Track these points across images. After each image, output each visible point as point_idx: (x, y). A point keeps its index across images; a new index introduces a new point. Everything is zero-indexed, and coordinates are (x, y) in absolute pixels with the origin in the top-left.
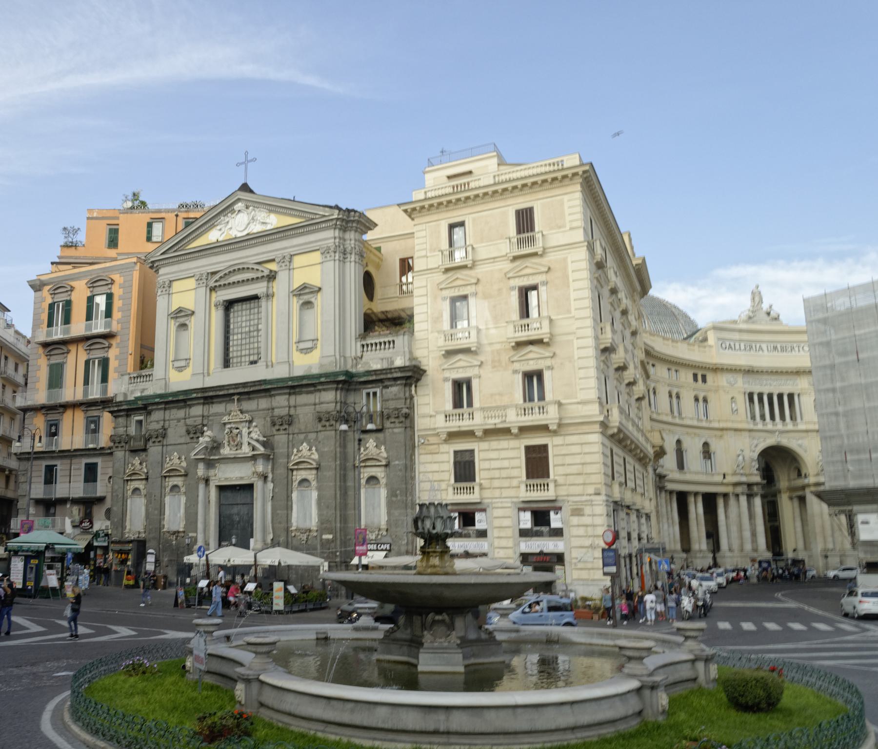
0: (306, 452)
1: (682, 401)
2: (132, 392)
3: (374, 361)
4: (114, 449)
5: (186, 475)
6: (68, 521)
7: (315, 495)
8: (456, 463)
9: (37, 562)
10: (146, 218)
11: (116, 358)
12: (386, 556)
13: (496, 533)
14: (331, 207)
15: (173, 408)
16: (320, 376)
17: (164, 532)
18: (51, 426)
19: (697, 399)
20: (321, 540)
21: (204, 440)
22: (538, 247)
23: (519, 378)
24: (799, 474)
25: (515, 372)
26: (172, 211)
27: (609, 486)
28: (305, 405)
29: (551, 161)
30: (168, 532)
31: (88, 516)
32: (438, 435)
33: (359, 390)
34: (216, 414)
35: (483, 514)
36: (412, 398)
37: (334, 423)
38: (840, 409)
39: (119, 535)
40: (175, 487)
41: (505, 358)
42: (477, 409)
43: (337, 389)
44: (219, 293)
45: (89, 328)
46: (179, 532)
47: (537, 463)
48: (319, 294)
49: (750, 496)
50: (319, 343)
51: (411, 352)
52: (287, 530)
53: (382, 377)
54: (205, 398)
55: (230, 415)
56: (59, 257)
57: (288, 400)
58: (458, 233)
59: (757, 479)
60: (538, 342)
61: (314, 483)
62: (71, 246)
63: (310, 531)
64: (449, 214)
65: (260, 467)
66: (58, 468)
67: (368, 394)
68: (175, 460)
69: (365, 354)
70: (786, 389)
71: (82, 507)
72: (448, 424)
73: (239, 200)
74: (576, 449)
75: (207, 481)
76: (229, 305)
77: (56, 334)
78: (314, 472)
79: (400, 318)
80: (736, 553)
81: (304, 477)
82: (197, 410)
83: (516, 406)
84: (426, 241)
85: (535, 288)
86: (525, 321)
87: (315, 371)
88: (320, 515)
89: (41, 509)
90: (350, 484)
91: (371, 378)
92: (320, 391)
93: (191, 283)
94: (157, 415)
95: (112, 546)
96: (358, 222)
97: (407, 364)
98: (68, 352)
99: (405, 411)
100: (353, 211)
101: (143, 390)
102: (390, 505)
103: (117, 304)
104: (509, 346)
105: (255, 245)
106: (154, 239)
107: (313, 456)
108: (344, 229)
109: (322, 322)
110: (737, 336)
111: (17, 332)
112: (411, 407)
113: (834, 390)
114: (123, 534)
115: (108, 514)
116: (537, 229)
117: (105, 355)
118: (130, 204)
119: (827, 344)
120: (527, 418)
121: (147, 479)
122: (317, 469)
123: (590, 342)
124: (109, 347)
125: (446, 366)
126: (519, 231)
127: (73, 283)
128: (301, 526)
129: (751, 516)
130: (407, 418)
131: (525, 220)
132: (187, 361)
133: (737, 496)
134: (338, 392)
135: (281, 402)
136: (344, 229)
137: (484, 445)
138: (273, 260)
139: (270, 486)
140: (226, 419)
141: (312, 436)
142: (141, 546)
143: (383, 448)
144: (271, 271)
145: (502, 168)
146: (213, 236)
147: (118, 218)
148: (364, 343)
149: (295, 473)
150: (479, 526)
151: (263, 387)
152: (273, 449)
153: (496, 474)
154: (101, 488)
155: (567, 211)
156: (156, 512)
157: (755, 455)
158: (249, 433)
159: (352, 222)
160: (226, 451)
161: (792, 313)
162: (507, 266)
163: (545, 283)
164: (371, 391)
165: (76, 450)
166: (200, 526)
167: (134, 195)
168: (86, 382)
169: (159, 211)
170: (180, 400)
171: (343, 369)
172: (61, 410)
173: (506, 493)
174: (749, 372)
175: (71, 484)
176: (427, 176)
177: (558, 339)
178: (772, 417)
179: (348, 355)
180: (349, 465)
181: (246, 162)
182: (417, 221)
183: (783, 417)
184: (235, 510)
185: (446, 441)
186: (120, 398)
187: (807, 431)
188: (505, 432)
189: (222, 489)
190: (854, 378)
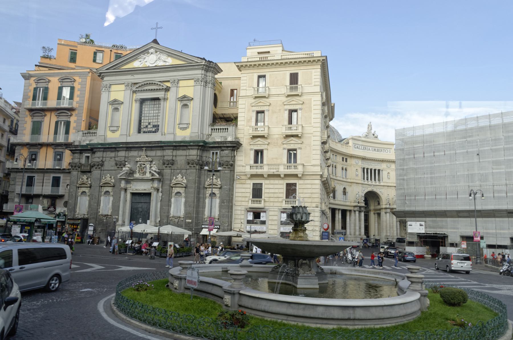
1: (337, 169)
2: (84, 141)
3: (217, 137)
4: (72, 170)
5: (114, 186)
6: (40, 207)
7: (183, 200)
8: (253, 189)
9: (29, 228)
10: (94, 49)
11: (75, 122)
12: (217, 232)
13: (270, 222)
14: (201, 58)
15: (108, 151)
16: (191, 142)
17: (99, 215)
18: (32, 155)
19: (343, 169)
20: (186, 222)
21: (126, 169)
22: (299, 92)
23: (286, 152)
24: (379, 204)
25: (284, 149)
26: (108, 48)
27: (321, 203)
28: (181, 156)
29: (306, 53)
30: (102, 215)
31: (53, 205)
32: (246, 175)
33: (209, 150)
34: (132, 156)
35: (265, 213)
36: (235, 156)
37: (195, 165)
38: (405, 177)
39: (72, 215)
40: (107, 192)
41: (280, 142)
42: (266, 165)
43: (198, 149)
44: (138, 94)
45: (58, 104)
46: (108, 215)
48: (192, 101)
49: (360, 212)
50: (190, 126)
51: (235, 135)
52: (168, 217)
53: (221, 145)
54: (127, 148)
55: (140, 157)
56: (39, 63)
57: (172, 152)
58: (261, 80)
59: (363, 205)
60: (296, 136)
61: (183, 194)
62: (47, 58)
63: (180, 217)
64: (259, 71)
65: (156, 184)
66: (36, 178)
67: (213, 153)
68: (108, 178)
69: (213, 133)
70: (377, 168)
71: (49, 200)
72: (251, 170)
73: (152, 47)
74: (309, 186)
75: (126, 190)
76: (143, 101)
77: (63, 104)
78: (184, 189)
79: (230, 118)
80: (353, 236)
81: (178, 191)
82: (122, 154)
83: (284, 165)
84: (246, 83)
85: (296, 111)
86: (290, 126)
87: (187, 139)
88: (185, 210)
89: (23, 200)
90: (201, 196)
91: (215, 145)
92: (189, 149)
93: (123, 87)
94: (99, 154)
95: (68, 221)
96: (214, 68)
97: (234, 140)
98: (45, 115)
99: (231, 162)
100: (212, 62)
101: (91, 140)
102: (221, 207)
103: (77, 93)
104: (282, 137)
105: (159, 72)
106: (97, 61)
107: (183, 181)
108: (207, 71)
109: (192, 116)
110: (360, 143)
111: (6, 101)
112: (234, 161)
113: (403, 169)
114: (74, 215)
115: (66, 204)
116: (299, 84)
117: (68, 120)
118: (84, 40)
119: (403, 150)
120: (288, 170)
121: (90, 187)
122: (185, 187)
123: (319, 138)
124: (71, 116)
125: (252, 143)
126: (291, 84)
127: (50, 78)
128: (175, 215)
129: (360, 220)
130: (231, 166)
131: (294, 79)
132: (118, 126)
133: (355, 211)
134: (199, 151)
135: (168, 153)
136: (207, 71)
137: (267, 182)
138: (169, 81)
139: (160, 194)
140: (138, 159)
141: (184, 171)
142: (85, 222)
143: (219, 179)
144: (167, 87)
145: (284, 52)
146: (136, 64)
147: (76, 47)
148: (213, 128)
149: (173, 189)
150: (262, 219)
151: (160, 145)
152: (163, 176)
153: (272, 195)
154: (62, 190)
155: (313, 77)
156: (95, 204)
157: (363, 195)
158: (151, 167)
159: (211, 68)
160: (137, 175)
161: (387, 134)
162: (284, 99)
163: (301, 109)
164: (215, 152)
165: (47, 169)
166: (121, 212)
167: (87, 35)
168: (56, 133)
169: (101, 47)
170: (114, 147)
171: (201, 140)
172: (39, 147)
173: (276, 204)
174: (364, 159)
175: (43, 187)
176: (248, 50)
177: (305, 135)
178: (371, 179)
179: (204, 133)
180: (202, 186)
181: (157, 28)
182: (243, 72)
183: (375, 180)
184: (140, 205)
185: (249, 178)
186: (77, 143)
187: (384, 186)
188: (277, 176)
189: (133, 194)
190: (411, 165)
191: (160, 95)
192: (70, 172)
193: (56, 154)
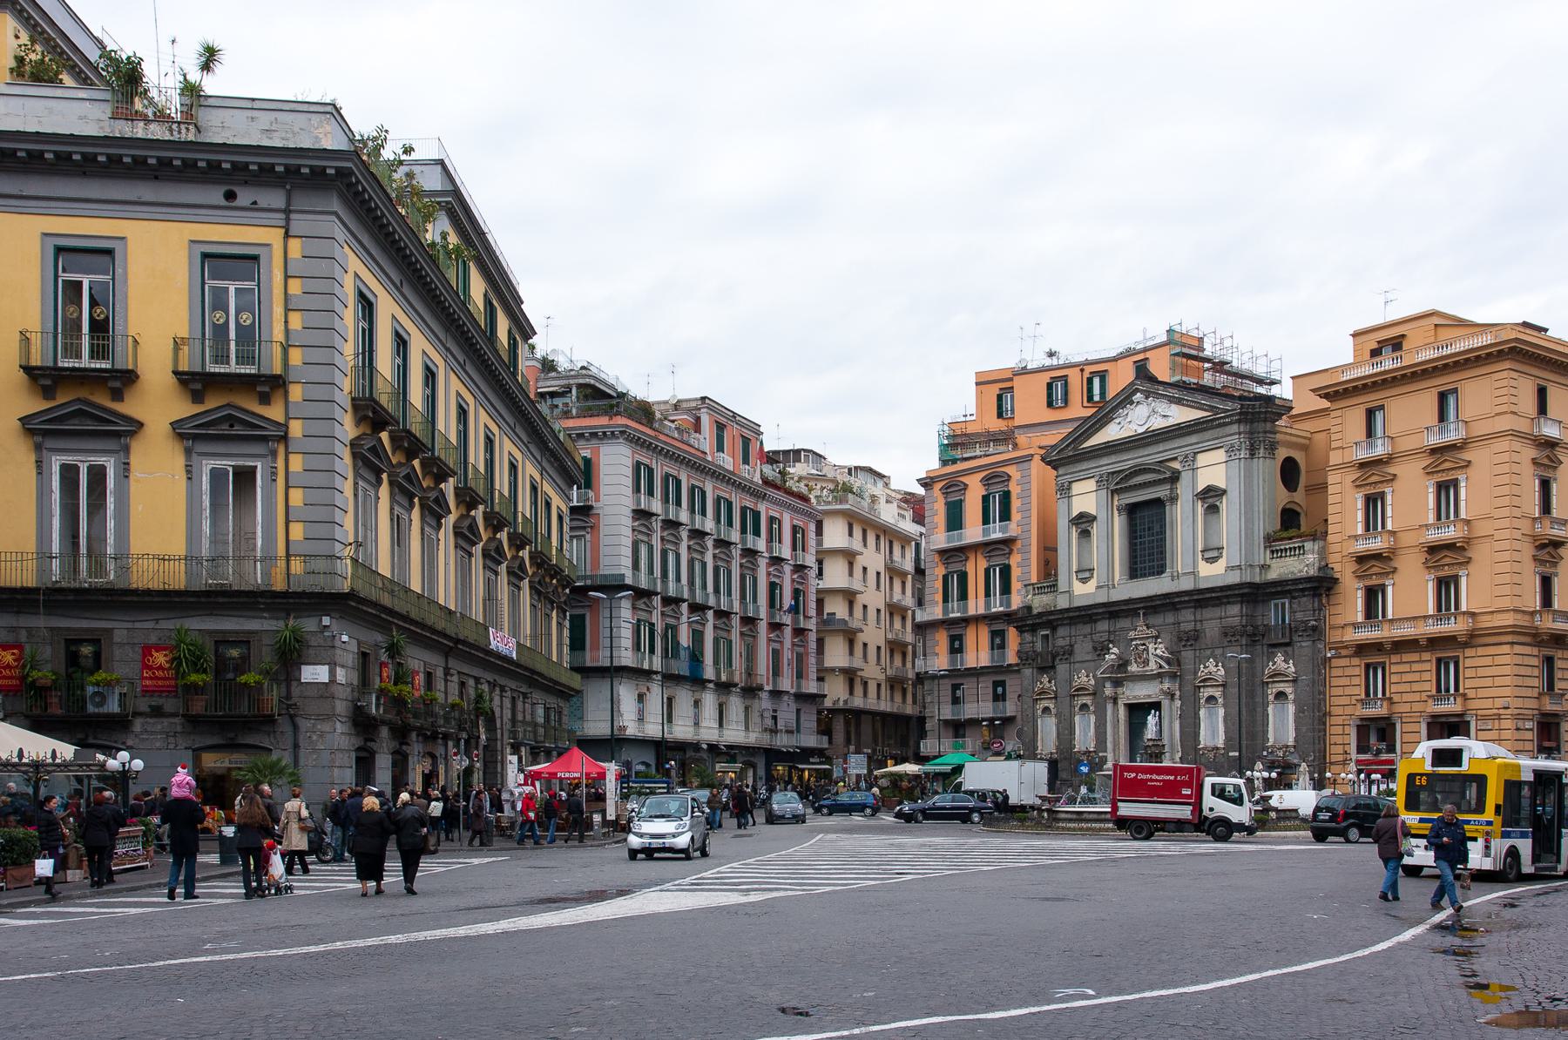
0: (1214, 668)
7: (1221, 712)
34: (1122, 629)
40: (1084, 707)
52: (1196, 750)
68: (1083, 679)
73: (1137, 390)
75: (1115, 700)
82: (1103, 626)
90: (1259, 699)
94: (1062, 631)
135: (1187, 618)
139: (1178, 703)
140: (1132, 634)
141: (1218, 652)
166: (1109, 745)
180: (1258, 680)
191: (1161, 492)
192: (1018, 671)
193: (994, 634)
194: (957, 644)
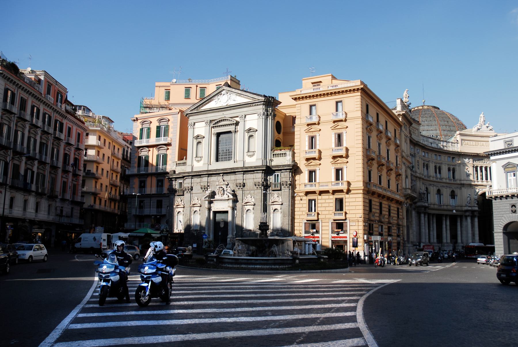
34: (213, 181)
47: (340, 204)
73: (224, 90)
76: (218, 135)
82: (205, 179)
84: (300, 112)
93: (203, 124)
137: (320, 197)
144: (237, 121)
146: (211, 105)
170: (199, 175)
191: (232, 128)
192: (168, 196)
194: (142, 184)
